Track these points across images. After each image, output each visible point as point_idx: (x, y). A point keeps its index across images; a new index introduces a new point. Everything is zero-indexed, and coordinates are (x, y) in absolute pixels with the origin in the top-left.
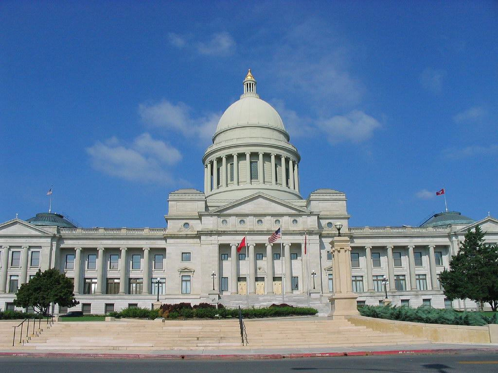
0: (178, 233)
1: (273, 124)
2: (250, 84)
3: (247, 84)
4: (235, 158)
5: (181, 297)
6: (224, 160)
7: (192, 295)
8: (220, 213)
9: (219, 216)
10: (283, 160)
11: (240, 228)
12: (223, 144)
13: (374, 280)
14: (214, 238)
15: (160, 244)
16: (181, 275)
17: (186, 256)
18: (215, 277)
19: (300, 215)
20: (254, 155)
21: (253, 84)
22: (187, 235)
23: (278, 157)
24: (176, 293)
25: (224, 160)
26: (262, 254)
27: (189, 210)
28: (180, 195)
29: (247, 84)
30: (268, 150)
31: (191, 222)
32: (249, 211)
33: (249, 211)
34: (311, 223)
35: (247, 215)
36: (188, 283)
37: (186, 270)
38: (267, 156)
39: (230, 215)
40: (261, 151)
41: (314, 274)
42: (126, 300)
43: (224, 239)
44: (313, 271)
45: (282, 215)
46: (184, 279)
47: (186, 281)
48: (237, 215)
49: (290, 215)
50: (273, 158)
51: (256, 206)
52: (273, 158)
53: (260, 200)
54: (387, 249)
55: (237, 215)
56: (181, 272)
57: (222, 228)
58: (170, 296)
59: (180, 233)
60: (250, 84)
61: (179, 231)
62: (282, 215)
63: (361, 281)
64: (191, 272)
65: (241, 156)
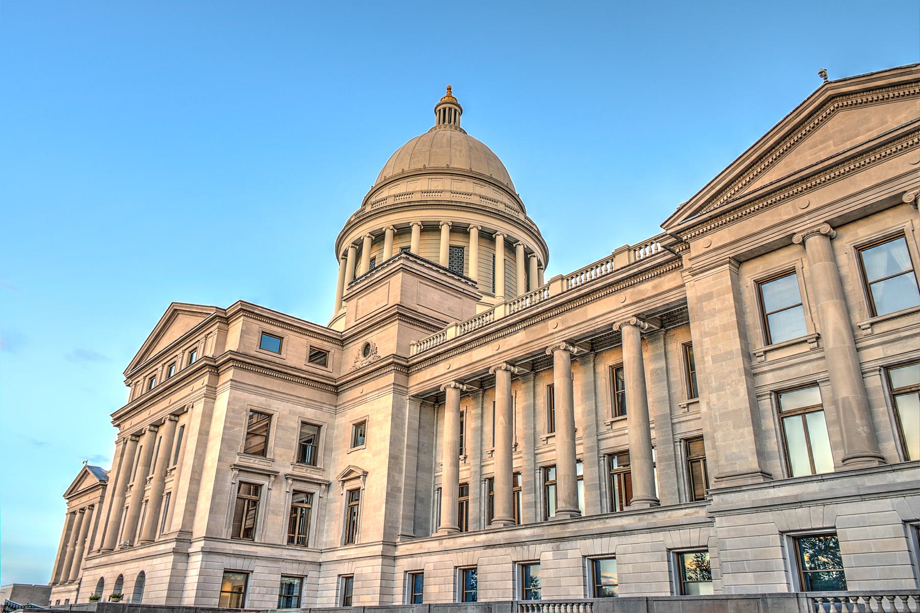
4: (415, 231)
6: (389, 234)
20: (460, 230)
21: (455, 111)
23: (510, 246)
30: (492, 223)
50: (500, 240)
52: (500, 240)
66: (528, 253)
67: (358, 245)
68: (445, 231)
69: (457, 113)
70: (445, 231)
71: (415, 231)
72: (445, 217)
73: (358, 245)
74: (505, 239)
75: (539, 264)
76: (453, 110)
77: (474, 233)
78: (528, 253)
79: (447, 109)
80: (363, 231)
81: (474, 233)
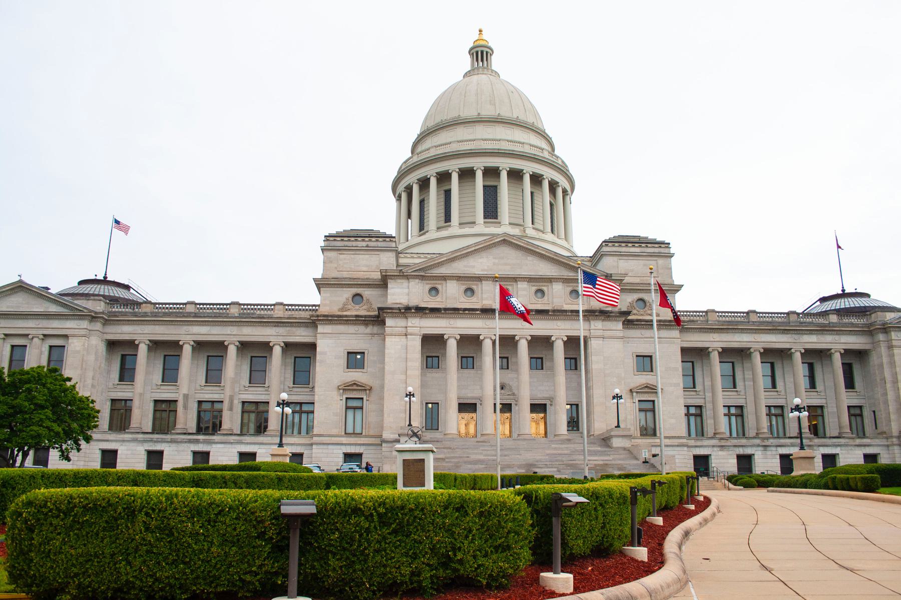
2: (482, 52)
4: (455, 177)
5: (344, 440)
6: (433, 182)
7: (366, 436)
8: (422, 274)
9: (422, 278)
12: (433, 153)
15: (301, 335)
16: (345, 397)
17: (354, 359)
18: (412, 399)
20: (492, 173)
21: (487, 53)
22: (357, 316)
23: (536, 179)
24: (335, 431)
25: (433, 182)
26: (507, 358)
27: (365, 269)
28: (346, 239)
31: (367, 293)
32: (482, 270)
33: (482, 270)
35: (479, 279)
36: (358, 412)
37: (355, 387)
39: (445, 278)
40: (505, 164)
43: (434, 325)
45: (550, 280)
46: (352, 403)
47: (355, 408)
48: (459, 278)
49: (566, 281)
50: (527, 179)
51: (496, 261)
52: (527, 179)
53: (505, 251)
55: (459, 278)
58: (321, 438)
59: (345, 313)
60: (482, 52)
61: (342, 310)
62: (550, 280)
63: (779, 415)
64: (366, 390)
65: (467, 174)
66: (553, 186)
67: (409, 190)
68: (479, 175)
69: (489, 54)
70: (479, 175)
71: (455, 177)
72: (479, 164)
73: (409, 190)
75: (565, 192)
77: (504, 175)
78: (553, 186)
80: (412, 179)
81: (504, 175)
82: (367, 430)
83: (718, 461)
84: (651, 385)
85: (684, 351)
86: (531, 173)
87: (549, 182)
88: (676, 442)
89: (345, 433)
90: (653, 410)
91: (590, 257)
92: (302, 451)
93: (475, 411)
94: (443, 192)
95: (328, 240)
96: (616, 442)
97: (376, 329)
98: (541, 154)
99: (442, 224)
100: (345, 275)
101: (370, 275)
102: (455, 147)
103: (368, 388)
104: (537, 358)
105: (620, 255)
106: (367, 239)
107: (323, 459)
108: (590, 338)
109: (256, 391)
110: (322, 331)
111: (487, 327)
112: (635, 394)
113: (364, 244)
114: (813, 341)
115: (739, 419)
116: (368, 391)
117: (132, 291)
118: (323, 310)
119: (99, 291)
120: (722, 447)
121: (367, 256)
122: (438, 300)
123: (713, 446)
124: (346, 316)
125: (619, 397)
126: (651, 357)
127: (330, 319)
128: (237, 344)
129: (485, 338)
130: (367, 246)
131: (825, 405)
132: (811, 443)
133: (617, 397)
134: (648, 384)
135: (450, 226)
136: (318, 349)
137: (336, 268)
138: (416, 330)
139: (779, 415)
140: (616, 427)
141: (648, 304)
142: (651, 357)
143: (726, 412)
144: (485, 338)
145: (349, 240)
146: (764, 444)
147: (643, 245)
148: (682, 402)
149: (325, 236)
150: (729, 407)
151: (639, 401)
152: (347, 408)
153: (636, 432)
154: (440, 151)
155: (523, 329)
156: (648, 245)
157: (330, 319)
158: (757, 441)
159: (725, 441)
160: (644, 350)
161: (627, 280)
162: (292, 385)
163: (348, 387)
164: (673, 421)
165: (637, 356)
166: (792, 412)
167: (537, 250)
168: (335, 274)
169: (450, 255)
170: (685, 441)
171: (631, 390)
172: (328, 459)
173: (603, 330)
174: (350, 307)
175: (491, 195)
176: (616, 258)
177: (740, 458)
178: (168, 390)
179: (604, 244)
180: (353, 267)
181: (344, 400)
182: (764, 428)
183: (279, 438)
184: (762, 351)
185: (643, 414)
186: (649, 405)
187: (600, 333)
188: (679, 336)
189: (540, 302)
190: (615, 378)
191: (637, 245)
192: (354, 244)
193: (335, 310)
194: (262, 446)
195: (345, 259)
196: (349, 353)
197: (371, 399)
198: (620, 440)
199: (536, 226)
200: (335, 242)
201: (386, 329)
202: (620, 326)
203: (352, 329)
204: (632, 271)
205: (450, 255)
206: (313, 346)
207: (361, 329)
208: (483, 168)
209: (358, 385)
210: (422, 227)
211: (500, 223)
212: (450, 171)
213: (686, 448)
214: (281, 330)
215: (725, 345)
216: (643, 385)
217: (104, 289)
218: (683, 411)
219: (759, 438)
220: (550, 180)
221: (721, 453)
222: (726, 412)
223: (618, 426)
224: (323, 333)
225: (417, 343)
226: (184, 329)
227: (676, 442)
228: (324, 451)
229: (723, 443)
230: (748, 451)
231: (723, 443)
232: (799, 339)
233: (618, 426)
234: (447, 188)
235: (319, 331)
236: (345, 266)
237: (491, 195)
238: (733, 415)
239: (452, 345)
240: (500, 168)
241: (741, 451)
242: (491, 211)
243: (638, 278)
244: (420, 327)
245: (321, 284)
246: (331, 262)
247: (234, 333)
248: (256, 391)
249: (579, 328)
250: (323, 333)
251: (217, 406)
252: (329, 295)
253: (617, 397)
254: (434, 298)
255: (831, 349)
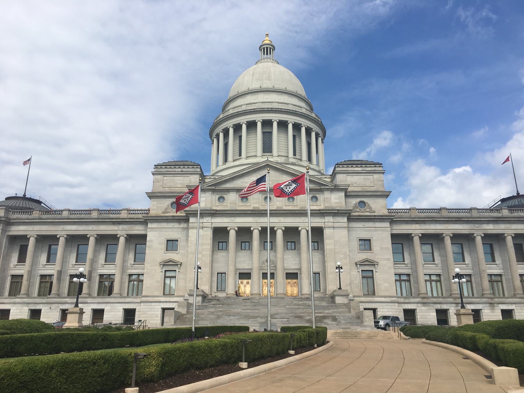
0: (163, 215)
1: (291, 88)
2: (267, 48)
3: (264, 48)
4: (244, 127)
5: (163, 299)
9: (214, 191)
10: (303, 130)
11: (241, 206)
12: (231, 112)
13: (426, 281)
14: (207, 220)
15: (138, 230)
16: (164, 270)
19: (321, 191)
20: (267, 124)
21: (270, 48)
23: (297, 127)
24: (156, 293)
25: (231, 131)
27: (180, 186)
28: (168, 167)
29: (264, 48)
34: (337, 201)
37: (171, 263)
38: (283, 125)
39: (228, 190)
40: (275, 117)
41: (339, 268)
42: (89, 305)
43: (220, 222)
44: (339, 263)
46: (168, 274)
47: (171, 277)
50: (290, 127)
52: (290, 127)
54: (444, 237)
56: (163, 265)
57: (219, 207)
59: (166, 215)
60: (267, 48)
61: (164, 212)
63: (428, 281)
65: (252, 125)
68: (259, 125)
70: (259, 125)
71: (244, 127)
72: (259, 118)
74: (293, 124)
76: (269, 49)
77: (275, 125)
79: (265, 49)
81: (275, 125)
82: (178, 291)
83: (422, 314)
84: (369, 259)
85: (394, 237)
86: (293, 123)
87: (306, 128)
88: (389, 300)
89: (164, 294)
90: (372, 277)
91: (330, 175)
92: (135, 308)
93: (297, 278)
94: (238, 137)
95: (156, 168)
96: (339, 300)
97: (185, 225)
98: (300, 111)
99: (238, 157)
100: (167, 190)
101: (183, 190)
102: (244, 108)
103: (179, 263)
104: (291, 242)
105: (347, 173)
106: (182, 167)
107: (148, 313)
108: (325, 228)
109: (109, 267)
110: (151, 227)
111: (255, 222)
112: (358, 266)
113: (180, 170)
114: (491, 228)
115: (439, 283)
116: (179, 266)
117: (42, 204)
118: (153, 213)
119: (19, 205)
120: (424, 304)
121: (182, 178)
122: (224, 205)
123: (418, 303)
124: (166, 217)
125: (340, 268)
126: (370, 240)
127: (158, 219)
128: (96, 236)
129: (254, 229)
130: (182, 171)
131: (503, 274)
132: (492, 302)
133: (339, 268)
134: (367, 259)
135: (240, 159)
136: (148, 238)
137: (161, 185)
138: (209, 225)
139: (428, 281)
140: (339, 289)
141: (367, 205)
142: (370, 240)
143: (398, 278)
144: (254, 229)
145: (170, 168)
146: (456, 302)
147: (364, 166)
148: (393, 271)
149: (155, 165)
150: (400, 275)
151: (362, 271)
152: (165, 277)
153: (360, 292)
154: (235, 111)
155: (279, 223)
156: (368, 166)
157: (158, 219)
158: (451, 300)
159: (427, 299)
160: (365, 235)
161: (350, 189)
162: (133, 263)
163: (165, 263)
164: (386, 285)
165: (360, 240)
166: (454, 279)
167: (289, 171)
168: (161, 189)
169: (231, 176)
170: (396, 299)
171: (356, 263)
172: (151, 313)
173: (334, 222)
174: (169, 210)
175: (267, 137)
176: (345, 175)
177: (438, 312)
178: (50, 268)
179: (336, 166)
180: (172, 185)
181: (164, 272)
182: (455, 290)
183: (76, 299)
184: (452, 235)
185: (365, 280)
186: (370, 274)
187: (331, 224)
188: (389, 226)
189: (291, 205)
190: (342, 255)
191: (359, 166)
192: (174, 170)
193: (160, 213)
194: (108, 305)
195: (167, 180)
196: (168, 241)
197: (181, 271)
198: (340, 298)
199: (297, 157)
200: (162, 169)
201: (189, 224)
202: (345, 219)
203: (170, 225)
204: (356, 183)
205: (231, 176)
206: (144, 237)
207: (176, 225)
208: (261, 121)
209: (173, 262)
210: (226, 160)
211: (272, 155)
212: (241, 124)
213: (397, 304)
214: (125, 227)
215: (423, 232)
216: (364, 259)
217: (23, 203)
218: (394, 278)
219: (452, 298)
220: (306, 127)
221: (423, 308)
222: (427, 278)
223: (340, 288)
224: (151, 228)
225: (208, 234)
226: (60, 227)
227: (389, 300)
228: (149, 307)
229: (425, 300)
230: (444, 307)
231: (425, 300)
232: (480, 227)
233: (340, 288)
234: (239, 135)
235: (148, 227)
236: (167, 184)
237: (267, 137)
238: (433, 281)
239: (232, 234)
240: (273, 121)
241: (439, 307)
242: (267, 148)
243: (360, 188)
244: (212, 223)
245: (151, 196)
246: (158, 182)
247: (94, 229)
248: (109, 267)
249: (318, 222)
250: (151, 228)
251: (111, 277)
252: (156, 203)
253: (339, 268)
254: (222, 203)
255: (505, 234)
